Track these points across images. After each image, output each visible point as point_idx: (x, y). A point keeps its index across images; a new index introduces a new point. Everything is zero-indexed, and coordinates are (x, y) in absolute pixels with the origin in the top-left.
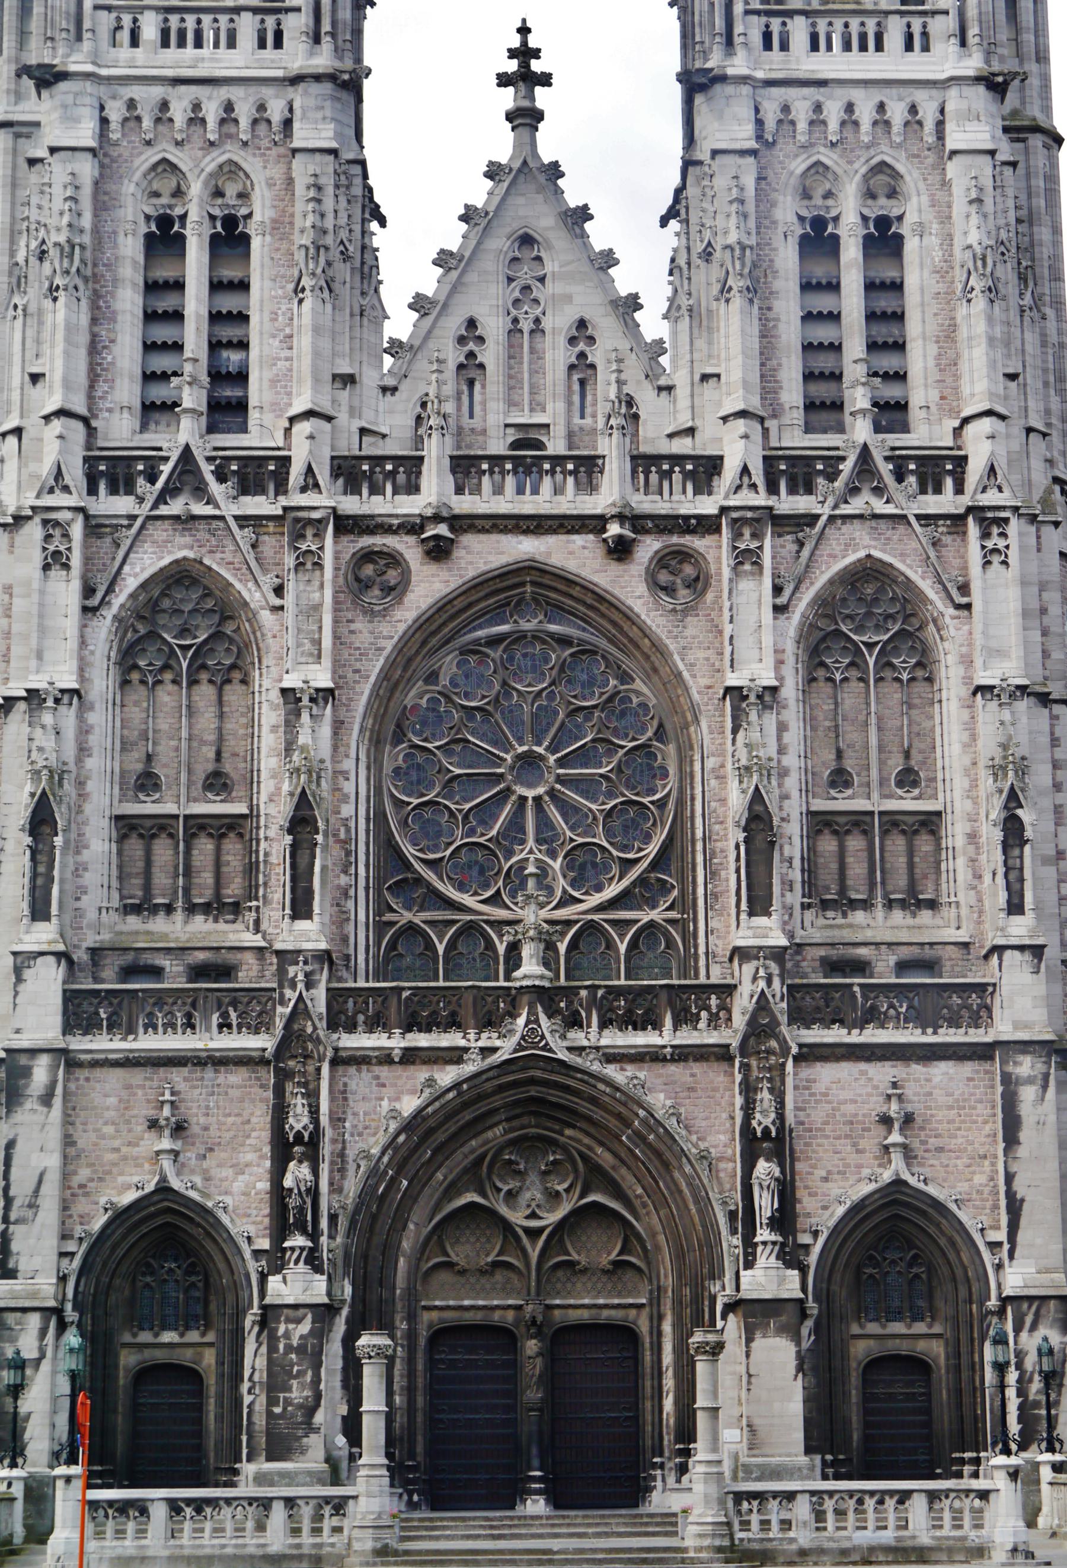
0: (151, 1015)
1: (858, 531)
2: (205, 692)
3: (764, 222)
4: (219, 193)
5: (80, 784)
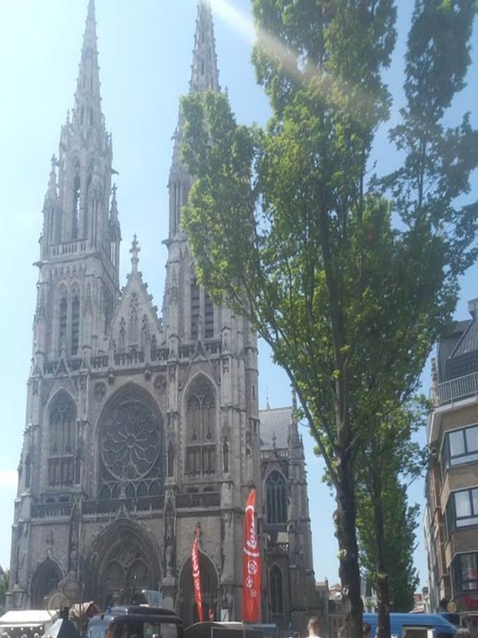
0: (47, 511)
1: (198, 366)
2: (66, 424)
3: (181, 282)
4: (74, 291)
5: (40, 450)
